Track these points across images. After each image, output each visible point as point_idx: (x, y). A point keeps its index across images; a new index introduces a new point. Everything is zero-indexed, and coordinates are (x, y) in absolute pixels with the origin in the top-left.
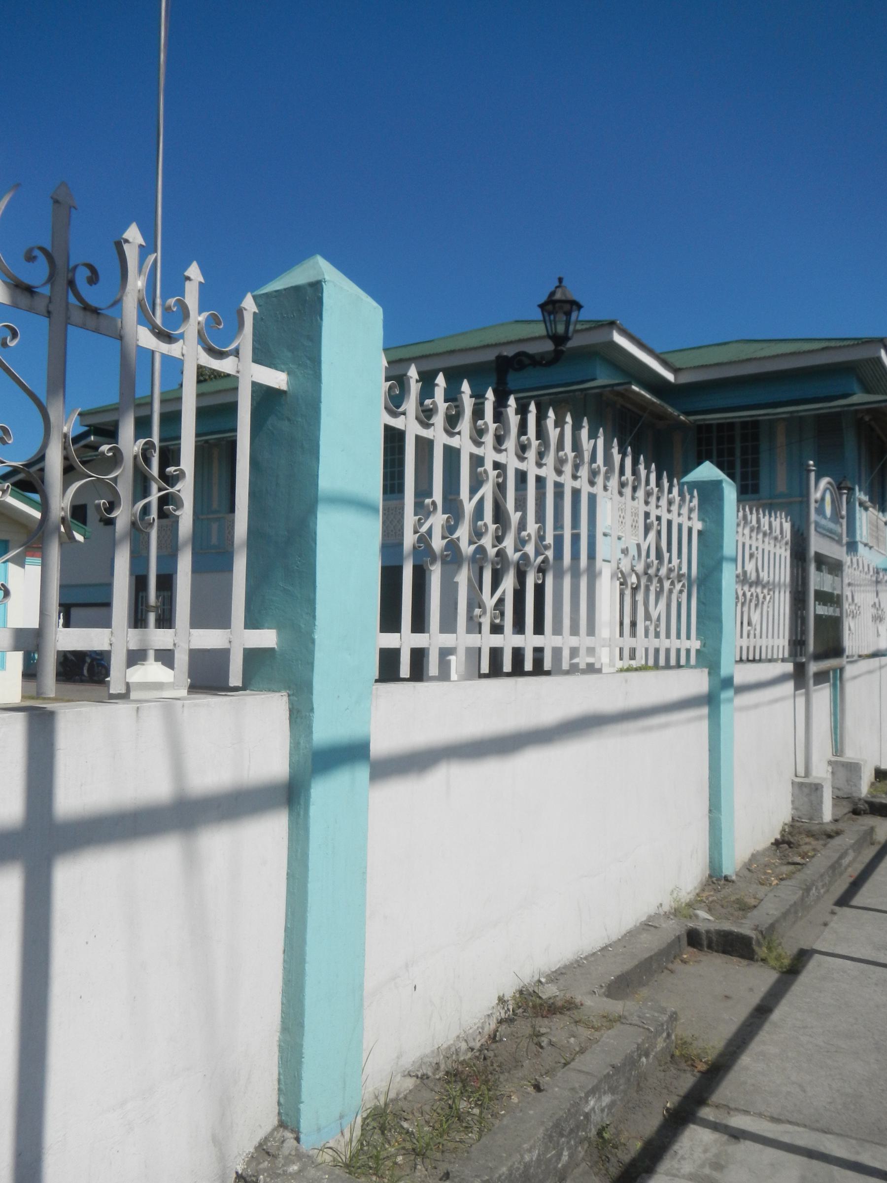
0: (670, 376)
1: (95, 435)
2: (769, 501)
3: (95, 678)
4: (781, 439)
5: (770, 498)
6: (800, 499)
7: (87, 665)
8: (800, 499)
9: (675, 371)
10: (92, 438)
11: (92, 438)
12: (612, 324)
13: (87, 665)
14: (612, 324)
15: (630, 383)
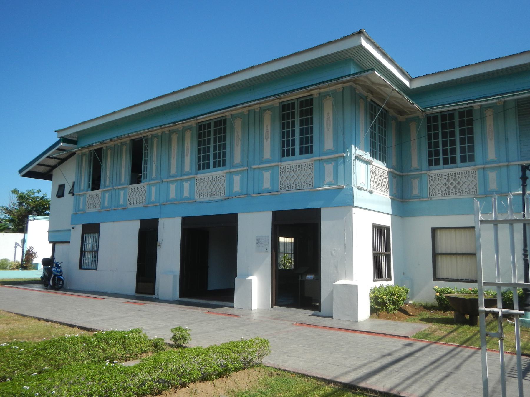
0: (407, 83)
1: (63, 142)
2: (483, 166)
3: (56, 287)
4: (490, 122)
5: (483, 164)
6: (507, 164)
7: (52, 279)
8: (507, 164)
9: (411, 80)
10: (62, 144)
11: (62, 144)
12: (360, 32)
13: (52, 279)
14: (360, 32)
15: (373, 69)
